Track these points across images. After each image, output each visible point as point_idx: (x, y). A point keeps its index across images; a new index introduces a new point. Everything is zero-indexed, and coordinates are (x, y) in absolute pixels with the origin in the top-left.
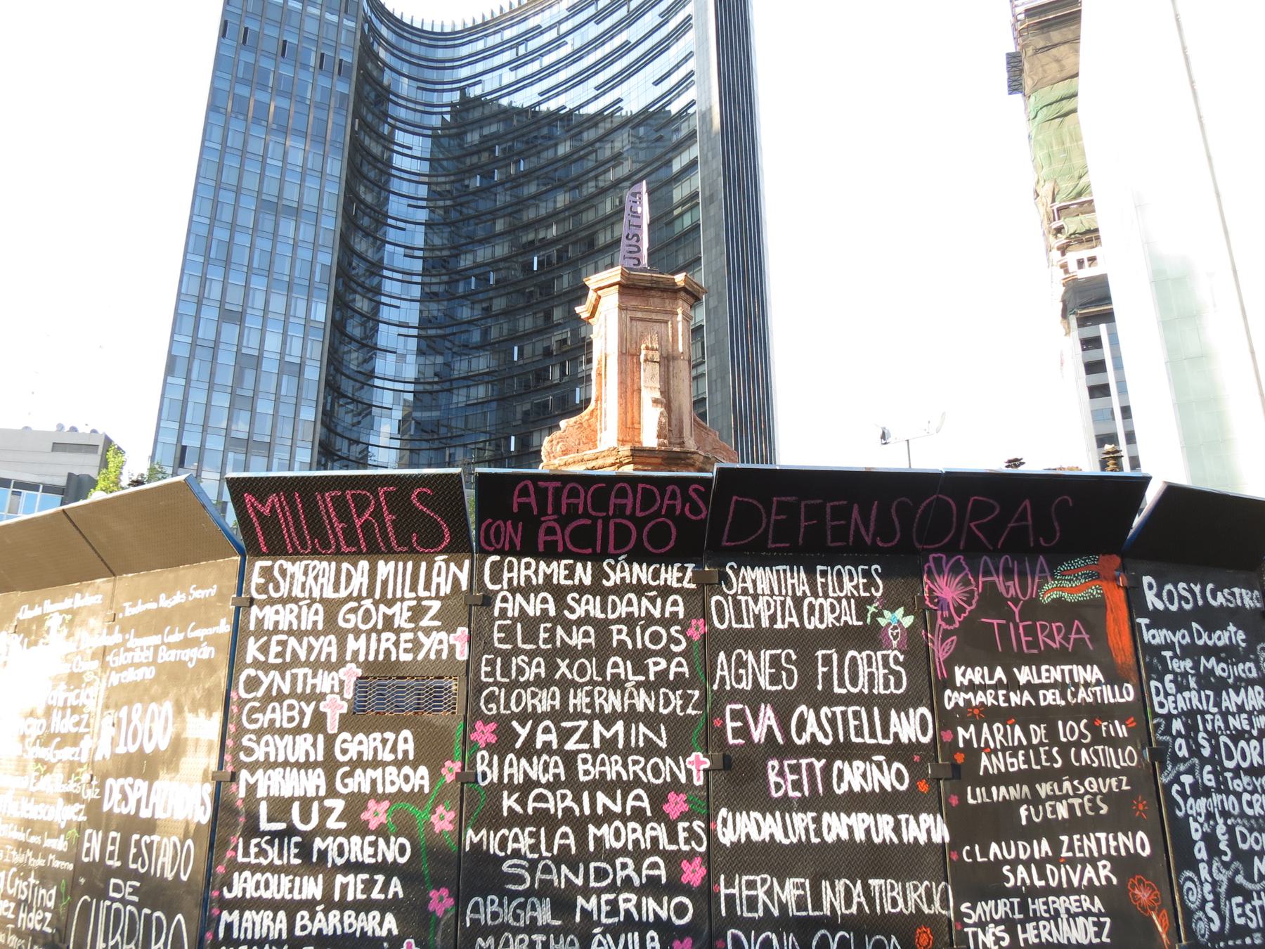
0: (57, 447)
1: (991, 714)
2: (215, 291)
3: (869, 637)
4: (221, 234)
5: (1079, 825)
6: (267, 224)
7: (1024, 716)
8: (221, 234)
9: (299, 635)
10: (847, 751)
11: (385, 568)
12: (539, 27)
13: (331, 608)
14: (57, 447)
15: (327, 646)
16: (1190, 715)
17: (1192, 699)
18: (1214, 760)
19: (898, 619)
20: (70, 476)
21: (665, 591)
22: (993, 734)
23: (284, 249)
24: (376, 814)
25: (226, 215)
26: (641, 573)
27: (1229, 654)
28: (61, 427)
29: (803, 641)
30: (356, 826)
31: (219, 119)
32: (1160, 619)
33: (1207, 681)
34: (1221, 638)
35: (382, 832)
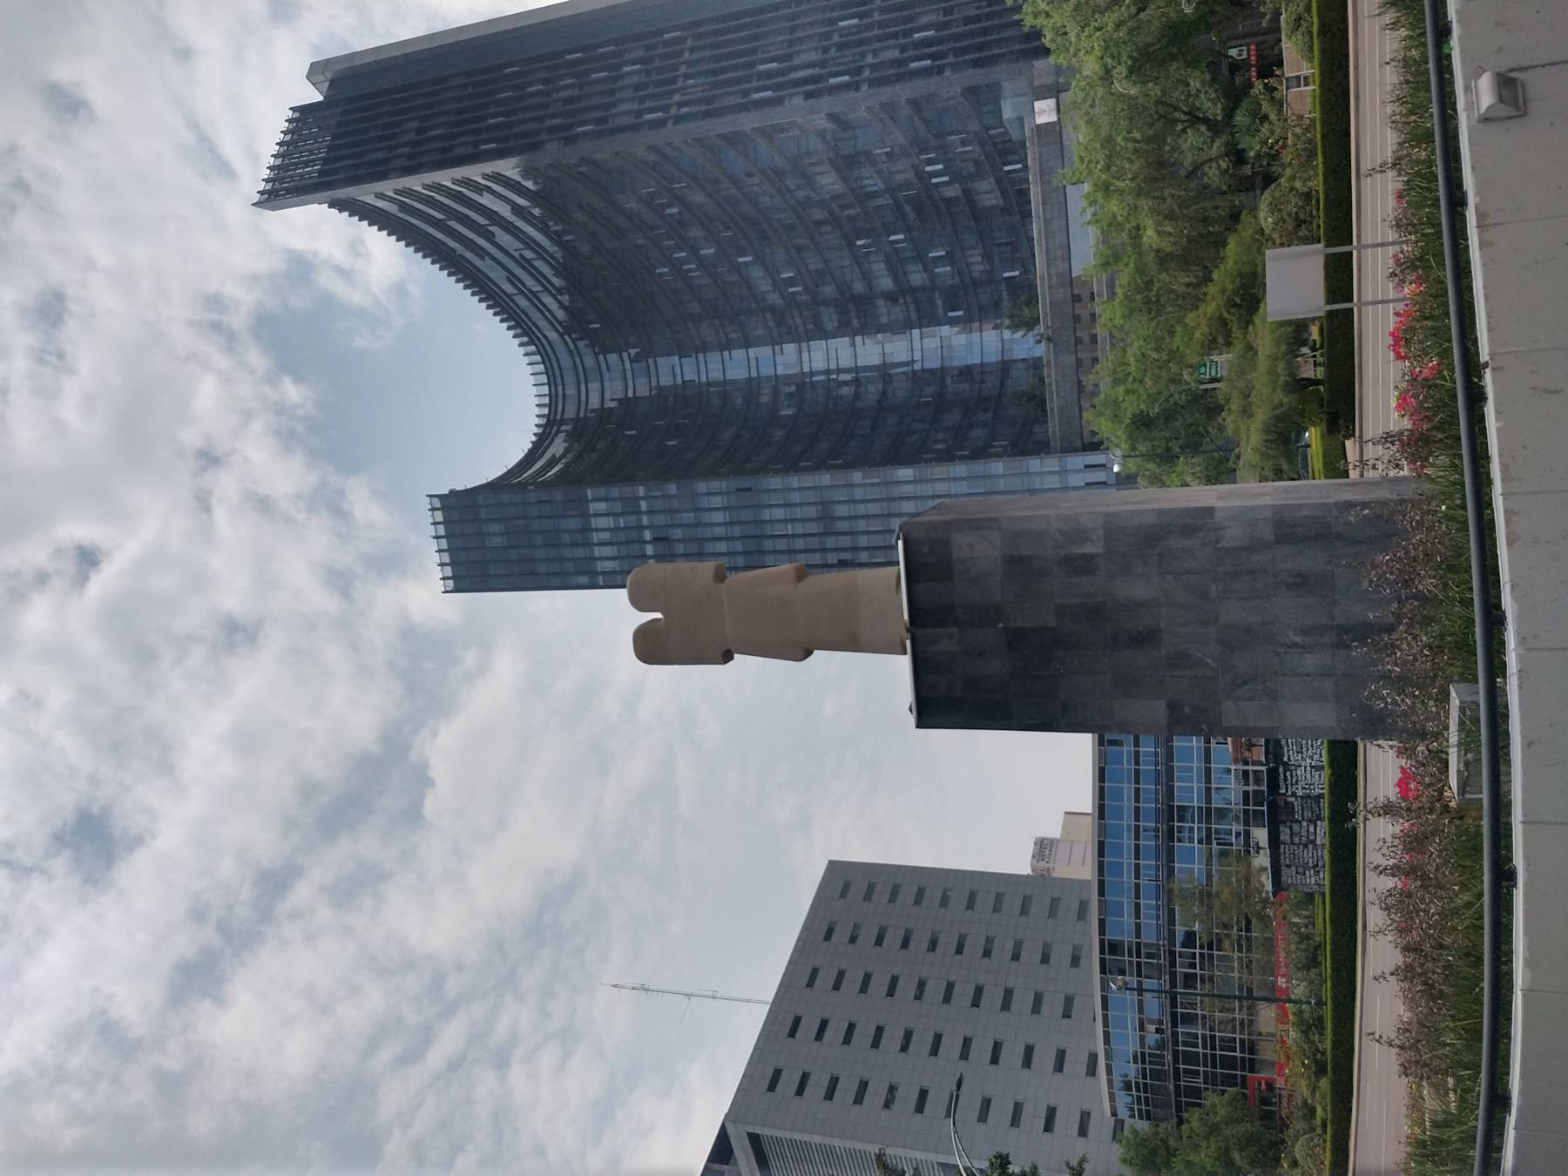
3: (1291, 828)
5: (1319, 807)
6: (843, 526)
10: (1308, 830)
12: (508, 279)
16: (1303, 788)
17: (1300, 787)
18: (1310, 785)
19: (1288, 824)
22: (1305, 814)
23: (861, 509)
26: (1282, 850)
27: (1292, 776)
29: (1292, 834)
32: (1287, 789)
34: (1289, 777)
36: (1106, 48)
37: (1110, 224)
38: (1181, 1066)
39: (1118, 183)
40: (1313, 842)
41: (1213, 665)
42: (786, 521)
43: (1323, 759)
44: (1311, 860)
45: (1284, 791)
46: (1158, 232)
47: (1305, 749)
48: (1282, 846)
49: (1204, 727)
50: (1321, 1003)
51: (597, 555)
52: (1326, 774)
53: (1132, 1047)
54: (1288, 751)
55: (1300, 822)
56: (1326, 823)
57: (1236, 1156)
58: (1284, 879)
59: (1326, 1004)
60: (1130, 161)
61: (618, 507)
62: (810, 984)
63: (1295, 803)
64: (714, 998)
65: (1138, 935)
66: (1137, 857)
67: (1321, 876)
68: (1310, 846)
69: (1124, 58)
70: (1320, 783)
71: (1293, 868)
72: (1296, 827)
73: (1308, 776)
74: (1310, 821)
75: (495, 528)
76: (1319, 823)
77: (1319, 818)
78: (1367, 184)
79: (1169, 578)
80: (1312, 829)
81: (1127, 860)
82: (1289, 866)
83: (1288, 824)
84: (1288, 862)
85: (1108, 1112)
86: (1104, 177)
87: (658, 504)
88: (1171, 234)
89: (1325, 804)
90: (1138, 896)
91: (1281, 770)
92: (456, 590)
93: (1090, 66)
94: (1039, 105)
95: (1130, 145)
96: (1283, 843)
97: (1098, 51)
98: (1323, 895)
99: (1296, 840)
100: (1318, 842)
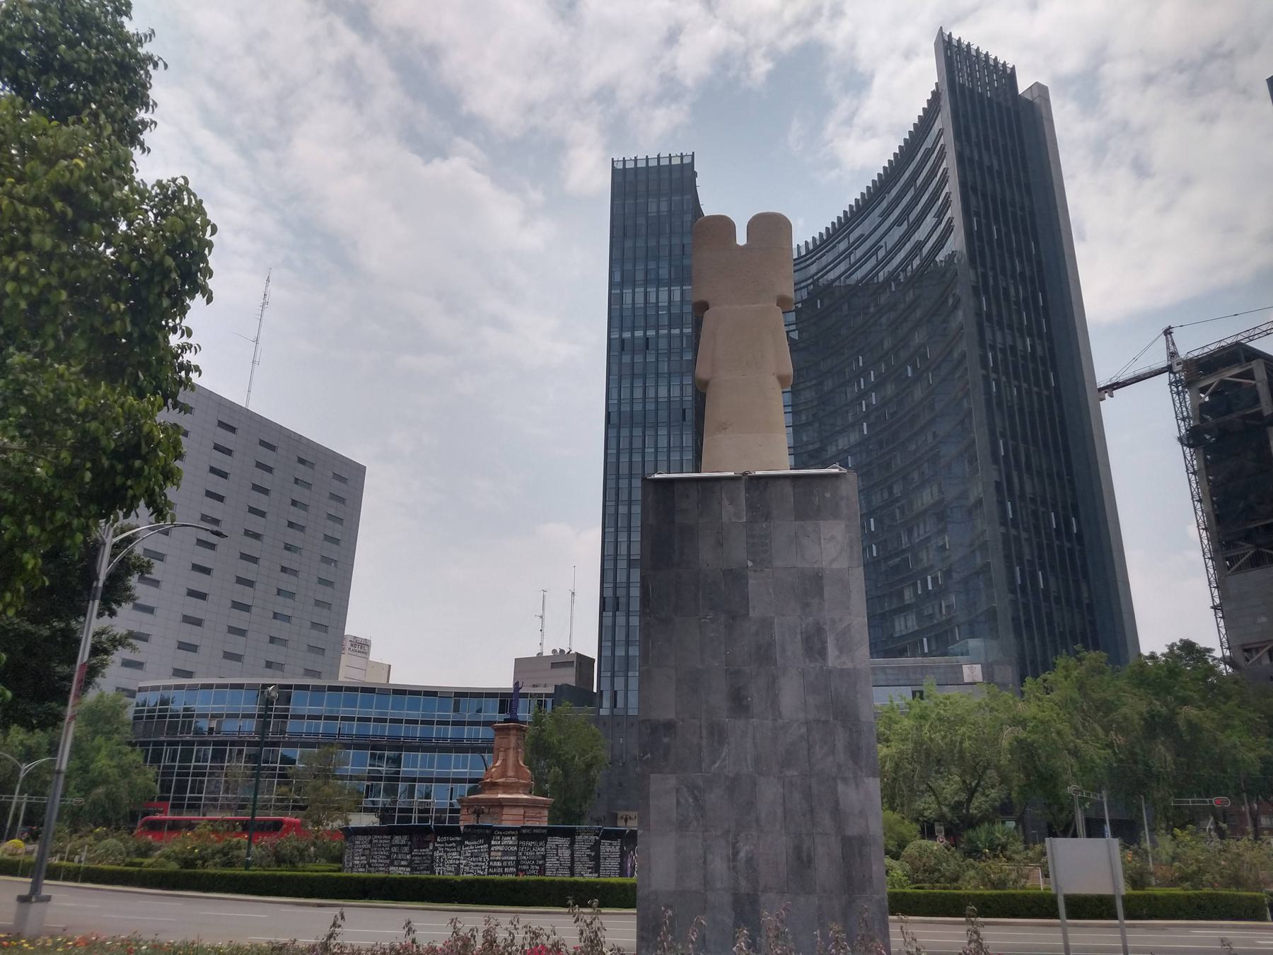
0: (554, 665)
1: (417, 855)
2: (623, 549)
3: (406, 845)
4: (623, 509)
5: (424, 870)
7: (420, 856)
8: (623, 509)
10: (403, 860)
12: (862, 235)
14: (554, 665)
16: (440, 857)
18: (443, 863)
19: (409, 843)
20: (556, 686)
22: (416, 858)
25: (624, 496)
27: (452, 847)
28: (554, 651)
29: (400, 845)
31: (613, 432)
32: (438, 843)
33: (444, 851)
34: (451, 845)
36: (1042, 722)
37: (890, 718)
38: (180, 747)
39: (927, 727)
40: (392, 864)
41: (713, 768)
42: (656, 448)
43: (465, 875)
44: (375, 861)
45: (438, 840)
46: (886, 756)
47: (474, 859)
49: (649, 755)
50: (247, 865)
51: (637, 290)
52: (451, 876)
53: (198, 707)
54: (473, 845)
55: (410, 853)
56: (408, 875)
57: (101, 790)
58: (359, 837)
59: (246, 869)
60: (944, 738)
61: (675, 310)
62: (263, 443)
63: (427, 850)
64: (253, 362)
65: (294, 717)
66: (360, 719)
67: (361, 870)
68: (388, 861)
69: (1034, 737)
70: (444, 872)
71: (369, 846)
72: (406, 849)
73: (451, 862)
74: (411, 861)
75: (664, 207)
76: (409, 869)
77: (413, 870)
78: (962, 931)
79: (803, 730)
80: (403, 863)
81: (357, 711)
82: (371, 842)
83: (409, 843)
84: (374, 841)
85: (142, 685)
86: (933, 716)
87: (676, 343)
88: (883, 767)
89: (424, 875)
90: (327, 718)
91: (458, 839)
92: (614, 170)
93: (1026, 709)
94: (978, 668)
95: (958, 738)
96: (392, 838)
97: (1040, 715)
98: (340, 870)
99: (395, 849)
100: (391, 868)
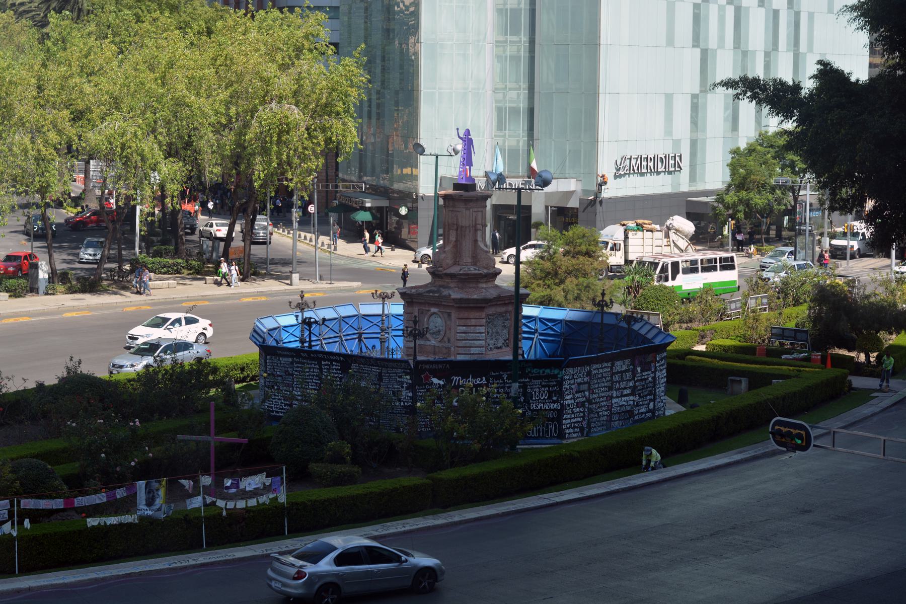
5: (647, 395)
9: (569, 380)
10: (625, 388)
11: (579, 368)
13: (573, 375)
15: (573, 381)
21: (608, 367)
22: (639, 383)
24: (579, 405)
26: (606, 365)
29: (622, 372)
30: (578, 407)
35: (581, 407)
44: (596, 396)
48: (609, 365)
55: (633, 379)
71: (587, 379)
72: (628, 375)
80: (626, 392)
82: (589, 373)
83: (632, 367)
84: (594, 372)
96: (613, 365)
99: (616, 378)
